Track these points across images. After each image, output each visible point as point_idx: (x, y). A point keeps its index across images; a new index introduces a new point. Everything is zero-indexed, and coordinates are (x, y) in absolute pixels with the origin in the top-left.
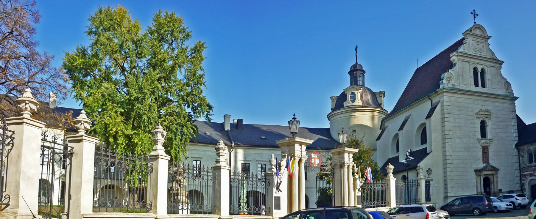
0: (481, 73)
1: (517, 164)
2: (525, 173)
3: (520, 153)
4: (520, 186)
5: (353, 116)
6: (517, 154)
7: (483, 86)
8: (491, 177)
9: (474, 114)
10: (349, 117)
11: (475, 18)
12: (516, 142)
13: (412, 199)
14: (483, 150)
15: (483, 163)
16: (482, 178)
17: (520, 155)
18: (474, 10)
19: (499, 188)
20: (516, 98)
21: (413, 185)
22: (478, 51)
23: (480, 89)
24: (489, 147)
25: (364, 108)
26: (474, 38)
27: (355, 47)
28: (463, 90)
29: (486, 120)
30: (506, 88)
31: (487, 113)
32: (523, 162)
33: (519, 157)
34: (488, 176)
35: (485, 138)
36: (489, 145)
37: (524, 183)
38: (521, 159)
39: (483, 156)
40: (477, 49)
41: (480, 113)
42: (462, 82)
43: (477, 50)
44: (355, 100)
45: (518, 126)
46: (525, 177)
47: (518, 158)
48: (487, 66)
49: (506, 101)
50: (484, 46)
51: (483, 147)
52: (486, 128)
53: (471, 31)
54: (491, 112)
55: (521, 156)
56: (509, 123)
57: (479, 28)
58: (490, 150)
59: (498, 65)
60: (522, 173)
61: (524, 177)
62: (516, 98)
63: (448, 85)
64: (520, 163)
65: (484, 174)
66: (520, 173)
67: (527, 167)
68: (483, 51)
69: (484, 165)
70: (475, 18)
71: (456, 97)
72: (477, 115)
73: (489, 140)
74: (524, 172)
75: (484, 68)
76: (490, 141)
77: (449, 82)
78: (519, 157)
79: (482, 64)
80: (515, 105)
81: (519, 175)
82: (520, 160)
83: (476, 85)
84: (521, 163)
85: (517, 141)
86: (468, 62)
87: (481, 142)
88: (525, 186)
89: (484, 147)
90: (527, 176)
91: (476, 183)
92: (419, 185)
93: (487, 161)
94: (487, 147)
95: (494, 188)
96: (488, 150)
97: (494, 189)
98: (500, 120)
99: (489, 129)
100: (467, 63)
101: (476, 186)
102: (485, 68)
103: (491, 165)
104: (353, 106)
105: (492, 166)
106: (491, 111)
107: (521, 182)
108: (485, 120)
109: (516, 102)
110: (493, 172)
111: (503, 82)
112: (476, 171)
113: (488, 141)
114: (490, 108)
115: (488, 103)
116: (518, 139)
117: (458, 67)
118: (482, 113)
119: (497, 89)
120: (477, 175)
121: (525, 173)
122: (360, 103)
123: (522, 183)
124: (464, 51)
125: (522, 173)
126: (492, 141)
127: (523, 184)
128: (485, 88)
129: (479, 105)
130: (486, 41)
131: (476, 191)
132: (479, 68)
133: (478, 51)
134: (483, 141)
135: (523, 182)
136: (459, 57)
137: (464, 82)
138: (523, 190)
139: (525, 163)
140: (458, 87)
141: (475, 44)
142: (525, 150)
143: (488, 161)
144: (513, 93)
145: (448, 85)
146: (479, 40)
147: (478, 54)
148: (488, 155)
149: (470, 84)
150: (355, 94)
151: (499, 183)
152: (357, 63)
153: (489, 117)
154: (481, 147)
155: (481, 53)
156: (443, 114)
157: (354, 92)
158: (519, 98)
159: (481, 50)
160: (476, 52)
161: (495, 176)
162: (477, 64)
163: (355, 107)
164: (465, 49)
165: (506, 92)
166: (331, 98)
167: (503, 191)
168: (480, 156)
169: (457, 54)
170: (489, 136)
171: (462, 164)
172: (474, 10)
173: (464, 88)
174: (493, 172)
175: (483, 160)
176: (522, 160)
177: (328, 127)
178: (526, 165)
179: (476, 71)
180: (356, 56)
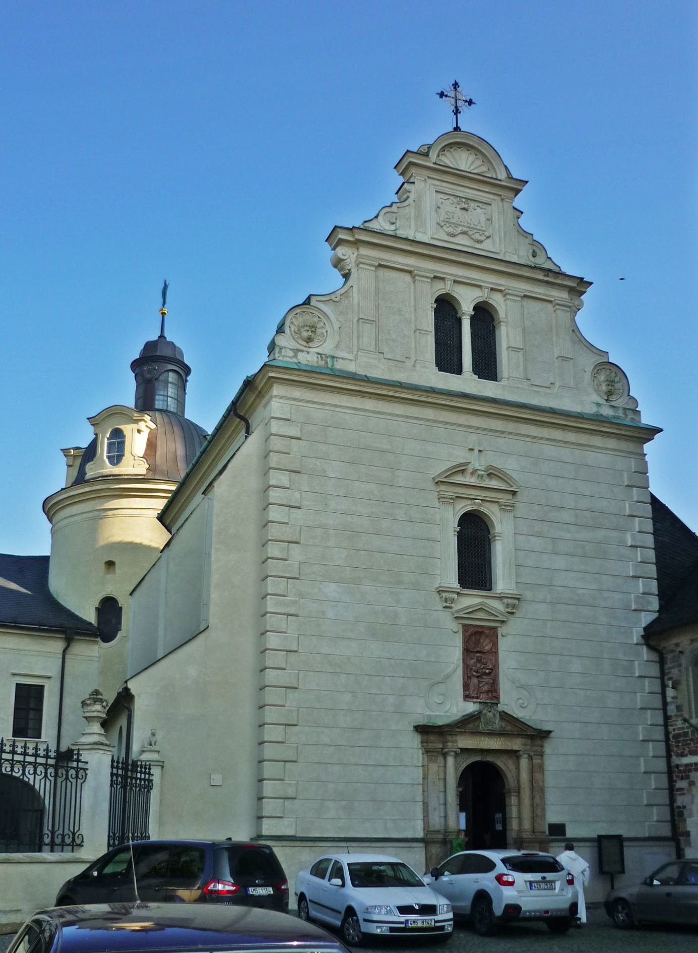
0: (473, 319)
1: (656, 717)
2: (686, 760)
3: (666, 666)
4: (668, 818)
5: (110, 513)
6: (654, 670)
8: (502, 763)
9: (431, 486)
10: (96, 513)
11: (457, 112)
12: (646, 619)
13: (61, 832)
14: (466, 641)
15: (467, 697)
16: (452, 768)
17: (666, 678)
18: (456, 85)
19: (553, 817)
20: (652, 432)
21: (46, 770)
22: (464, 233)
24: (500, 631)
25: (149, 483)
26: (445, 184)
27: (163, 285)
28: (367, 380)
29: (492, 512)
30: (604, 388)
31: (494, 483)
32: (679, 708)
33: (664, 686)
34: (490, 759)
35: (490, 589)
36: (503, 622)
37: (684, 807)
38: (670, 692)
39: (466, 667)
41: (458, 479)
42: (372, 348)
43: (460, 228)
44: (123, 455)
45: (660, 548)
46: (688, 777)
47: (658, 689)
48: (505, 296)
49: (597, 441)
50: (495, 217)
51: (466, 628)
52: (492, 544)
53: (426, 155)
54: (511, 478)
55: (670, 683)
56: (614, 534)
57: (469, 147)
58: (504, 645)
59: (564, 295)
60: (676, 760)
61: (682, 778)
62: (652, 432)
63: (296, 356)
64: (669, 713)
65: (462, 750)
66: (669, 757)
67: (693, 732)
68: (488, 237)
69: (471, 707)
70: (457, 112)
71: (336, 406)
72: (443, 488)
73: (500, 598)
74: (682, 755)
75: (491, 301)
76: (508, 606)
77: (311, 344)
78: (664, 686)
79: (480, 287)
80: (647, 458)
81: (662, 765)
82: (669, 700)
84: (673, 714)
85: (656, 615)
86: (410, 272)
87: (456, 607)
88: (689, 821)
89: (471, 630)
91: (420, 787)
92: (81, 773)
93: (488, 692)
94: (491, 628)
95: (520, 818)
96: (495, 644)
97: (520, 824)
98: (567, 516)
100: (407, 278)
101: (420, 798)
102: (497, 301)
103: (500, 707)
104: (112, 478)
105: (504, 716)
106: (514, 475)
107: (672, 800)
108: (483, 509)
109: (647, 447)
110: (516, 744)
111: (588, 362)
112: (423, 730)
113: (498, 605)
114: (510, 466)
115: (502, 442)
116: (661, 606)
117: (355, 289)
118: (473, 480)
119: (556, 389)
120: (427, 752)
121: (686, 760)
122: (141, 468)
123: (675, 805)
124: (393, 227)
125: (676, 760)
126: (514, 606)
127: (679, 807)
128: (496, 381)
130: (502, 200)
131: (420, 825)
134: (472, 599)
135: (680, 801)
136: (364, 251)
137: (385, 349)
138: (682, 838)
139: (687, 716)
140: (351, 368)
141: (450, 207)
144: (639, 412)
145: (300, 354)
146: (470, 193)
149: (413, 359)
150: (124, 436)
151: (551, 796)
152: (162, 336)
153: (505, 498)
154: (456, 626)
155: (480, 242)
156: (266, 471)
157: (121, 427)
158: (660, 430)
159: (481, 231)
160: (453, 235)
161: (524, 762)
162: (455, 281)
163: (118, 479)
164: (398, 223)
165: (598, 405)
166: (65, 451)
167: (570, 833)
168: (452, 667)
169: (353, 236)
170: (502, 581)
171: (347, 697)
172: (456, 85)
173: (376, 373)
174: (516, 744)
175: (466, 686)
176: (673, 698)
177: (44, 550)
178: (685, 720)
179: (456, 313)
180: (163, 314)
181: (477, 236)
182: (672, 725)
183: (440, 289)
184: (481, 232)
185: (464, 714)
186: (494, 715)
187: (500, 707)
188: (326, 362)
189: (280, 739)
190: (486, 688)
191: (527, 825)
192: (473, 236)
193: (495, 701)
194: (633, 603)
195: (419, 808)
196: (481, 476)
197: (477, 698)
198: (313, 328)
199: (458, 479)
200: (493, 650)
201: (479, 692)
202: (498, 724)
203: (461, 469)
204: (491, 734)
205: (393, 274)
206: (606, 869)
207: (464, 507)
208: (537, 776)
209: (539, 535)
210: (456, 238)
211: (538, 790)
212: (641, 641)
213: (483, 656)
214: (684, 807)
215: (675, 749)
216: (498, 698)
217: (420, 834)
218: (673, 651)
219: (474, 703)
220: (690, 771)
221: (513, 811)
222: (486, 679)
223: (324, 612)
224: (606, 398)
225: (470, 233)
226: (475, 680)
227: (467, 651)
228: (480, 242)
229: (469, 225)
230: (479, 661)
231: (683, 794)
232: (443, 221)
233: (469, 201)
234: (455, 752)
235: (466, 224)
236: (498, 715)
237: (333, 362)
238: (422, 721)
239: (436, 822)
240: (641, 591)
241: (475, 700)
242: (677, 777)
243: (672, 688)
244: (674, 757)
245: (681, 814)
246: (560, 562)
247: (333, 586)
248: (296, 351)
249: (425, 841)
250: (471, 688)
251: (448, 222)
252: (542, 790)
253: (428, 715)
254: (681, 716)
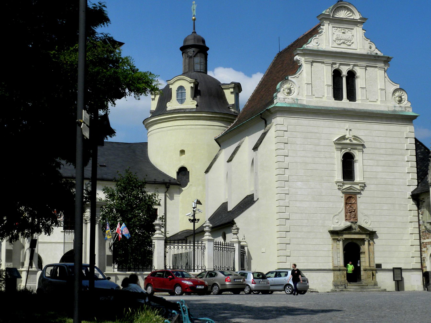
2: (425, 241)
3: (420, 207)
7: (352, 96)
8: (358, 243)
15: (346, 220)
19: (377, 261)
22: (344, 43)
32: (423, 222)
33: (419, 213)
34: (354, 241)
37: (425, 258)
38: (420, 216)
40: (341, 40)
43: (342, 41)
46: (426, 247)
52: (355, 164)
60: (422, 241)
63: (284, 100)
64: (420, 223)
66: (420, 239)
69: (348, 224)
73: (357, 184)
74: (424, 239)
76: (360, 186)
81: (418, 242)
82: (420, 218)
90: (428, 246)
98: (382, 151)
99: (358, 167)
101: (331, 255)
103: (358, 223)
105: (360, 227)
107: (421, 255)
110: (363, 237)
113: (358, 187)
121: (425, 241)
123: (422, 257)
124: (317, 45)
125: (422, 241)
127: (423, 258)
132: (344, 70)
135: (424, 255)
142: (424, 202)
145: (286, 99)
148: (357, 208)
155: (350, 45)
160: (340, 44)
167: (383, 267)
168: (341, 209)
170: (358, 177)
174: (363, 237)
175: (346, 216)
181: (349, 43)
182: (421, 228)
184: (350, 41)
185: (346, 226)
186: (356, 226)
187: (358, 223)
188: (295, 102)
189: (284, 237)
190: (353, 216)
192: (347, 43)
193: (356, 221)
194: (407, 183)
195: (331, 259)
197: (350, 220)
200: (355, 203)
202: (358, 230)
203: (343, 138)
207: (344, 151)
210: (341, 45)
212: (411, 197)
213: (352, 205)
214: (425, 258)
215: (422, 237)
216: (357, 220)
218: (422, 201)
219: (349, 222)
220: (427, 245)
221: (362, 259)
222: (353, 213)
223: (297, 192)
224: (398, 103)
225: (346, 42)
226: (349, 214)
228: (350, 45)
229: (345, 39)
231: (425, 253)
232: (336, 39)
233: (345, 29)
234: (343, 239)
235: (344, 39)
236: (357, 226)
237: (297, 101)
238: (332, 229)
240: (411, 178)
241: (349, 221)
242: (423, 247)
243: (421, 214)
244: (422, 240)
245: (424, 260)
246: (379, 169)
247: (300, 183)
248: (284, 99)
250: (348, 216)
253: (333, 227)
254: (424, 225)
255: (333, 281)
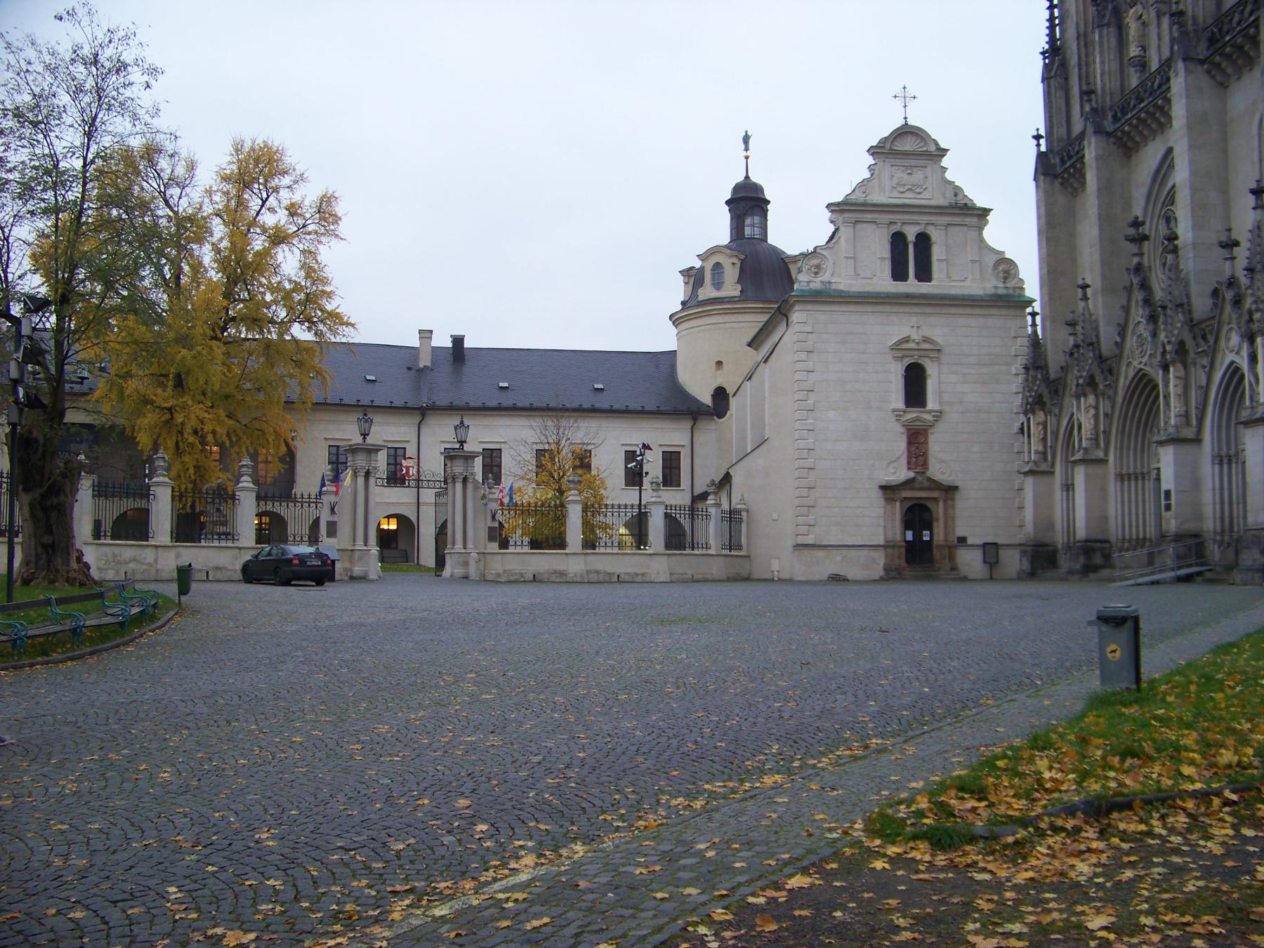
0: (915, 245)
8: (929, 504)
15: (909, 469)
19: (960, 532)
22: (910, 189)
23: (911, 285)
31: (926, 346)
34: (922, 502)
35: (925, 407)
39: (909, 451)
40: (904, 185)
41: (905, 346)
50: (929, 175)
51: (909, 430)
57: (912, 133)
69: (911, 474)
73: (929, 412)
83: (899, 273)
96: (926, 438)
101: (882, 524)
103: (929, 474)
105: (930, 480)
108: (920, 361)
110: (935, 494)
112: (884, 488)
113: (928, 417)
118: (912, 345)
126: (937, 416)
129: (901, 326)
132: (911, 233)
133: (910, 189)
134: (912, 414)
141: (900, 175)
143: (925, 465)
147: (909, 199)
148: (927, 450)
153: (935, 354)
154: (902, 430)
160: (902, 193)
161: (941, 504)
167: (969, 542)
170: (931, 404)
174: (935, 494)
175: (909, 463)
181: (918, 190)
183: (895, 229)
187: (929, 474)
191: (942, 538)
195: (881, 530)
196: (918, 343)
198: (818, 267)
199: (905, 346)
201: (916, 465)
203: (906, 340)
204: (921, 489)
205: (865, 225)
206: (987, 560)
207: (907, 361)
208: (950, 511)
209: (955, 373)
211: (950, 519)
216: (927, 469)
217: (882, 542)
222: (921, 458)
227: (910, 443)
230: (917, 448)
238: (884, 483)
239: (890, 536)
249: (885, 547)
251: (899, 184)
252: (953, 519)
255: (885, 564)
